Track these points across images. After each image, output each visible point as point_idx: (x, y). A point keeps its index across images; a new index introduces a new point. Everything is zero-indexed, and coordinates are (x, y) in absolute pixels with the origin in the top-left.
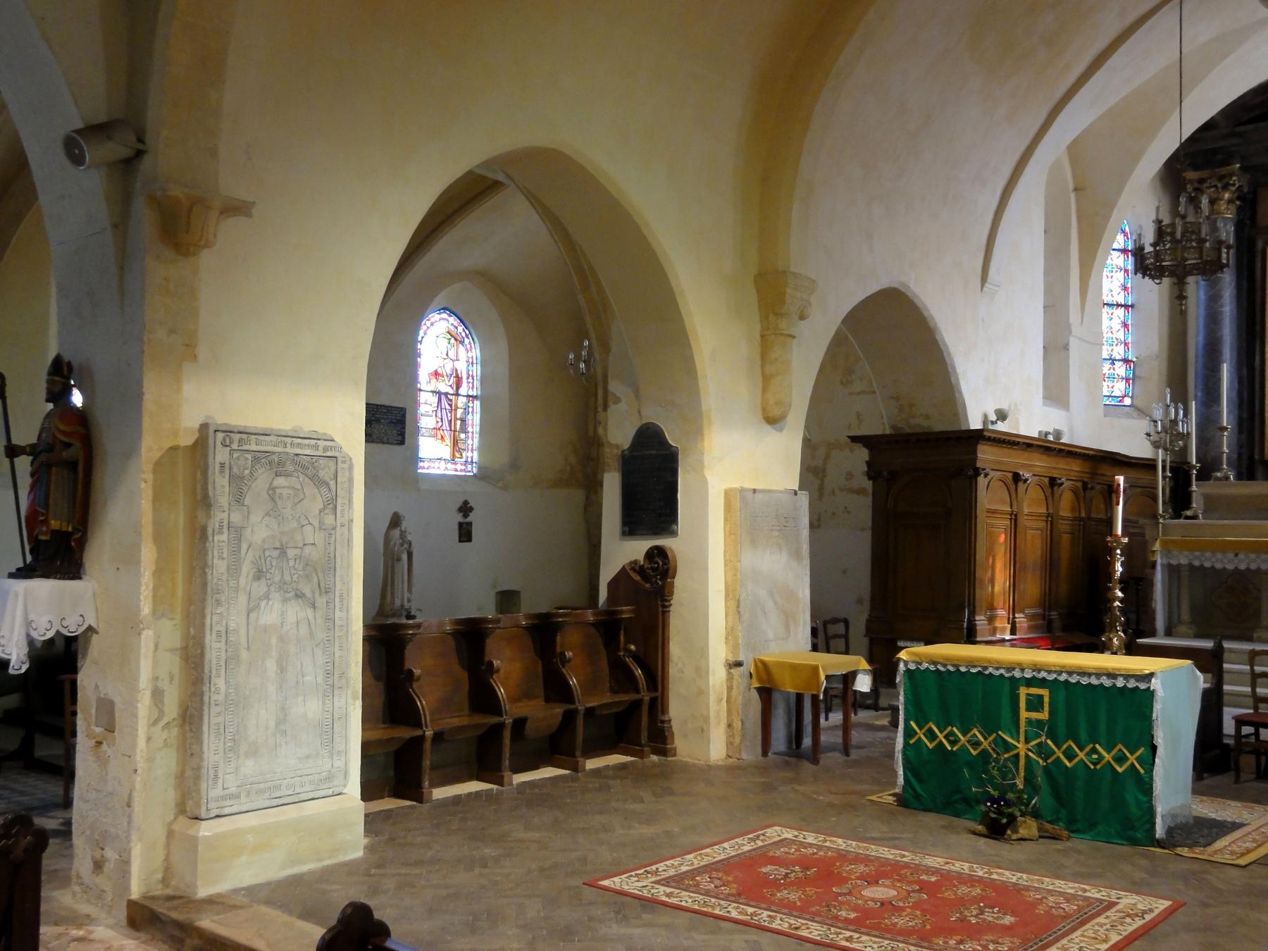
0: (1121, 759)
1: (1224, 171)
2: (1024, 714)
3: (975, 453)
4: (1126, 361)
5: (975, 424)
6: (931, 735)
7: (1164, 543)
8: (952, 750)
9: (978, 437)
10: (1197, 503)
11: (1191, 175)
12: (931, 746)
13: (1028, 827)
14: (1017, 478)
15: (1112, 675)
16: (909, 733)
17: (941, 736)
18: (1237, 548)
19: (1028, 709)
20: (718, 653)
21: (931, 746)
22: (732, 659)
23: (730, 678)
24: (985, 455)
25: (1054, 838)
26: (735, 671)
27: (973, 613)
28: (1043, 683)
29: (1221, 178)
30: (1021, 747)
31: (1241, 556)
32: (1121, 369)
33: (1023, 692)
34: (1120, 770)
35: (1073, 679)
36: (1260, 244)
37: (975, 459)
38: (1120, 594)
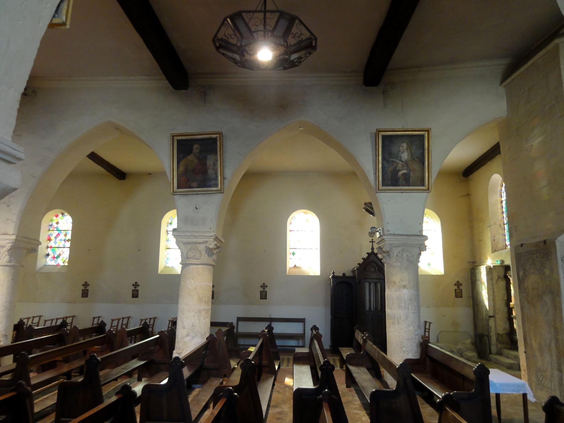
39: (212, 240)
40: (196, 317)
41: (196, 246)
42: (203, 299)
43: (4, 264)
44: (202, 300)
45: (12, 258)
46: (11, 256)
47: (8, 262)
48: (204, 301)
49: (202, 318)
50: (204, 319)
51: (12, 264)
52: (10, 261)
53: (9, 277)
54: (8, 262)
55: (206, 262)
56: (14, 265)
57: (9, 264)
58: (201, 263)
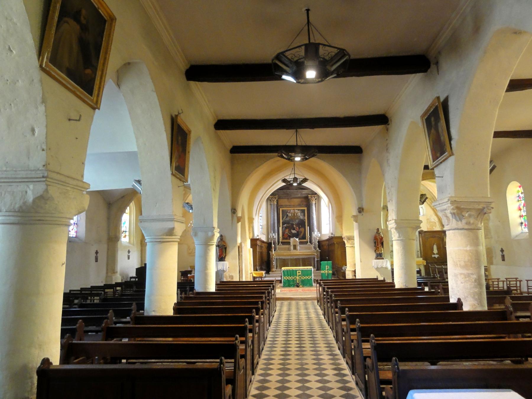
0: (309, 277)
1: (275, 196)
2: (298, 274)
3: (257, 242)
4: (261, 226)
5: (255, 238)
6: (286, 278)
7: (276, 255)
8: (290, 280)
9: (258, 239)
10: (277, 249)
11: (271, 197)
12: (286, 279)
13: (301, 286)
14: (259, 245)
15: (308, 268)
16: (284, 278)
17: (287, 278)
18: (286, 255)
19: (298, 273)
20: (249, 272)
21: (286, 279)
22: (250, 273)
23: (250, 275)
24: (258, 243)
25: (303, 287)
26: (251, 274)
27: (257, 267)
28: (300, 270)
29: (275, 197)
30: (298, 278)
31: (287, 256)
32: (261, 227)
33: (298, 271)
34: (309, 279)
35: (303, 269)
36: (279, 208)
37: (257, 243)
38: (274, 263)
39: (449, 205)
40: (453, 281)
41: (445, 213)
42: (458, 264)
43: (397, 239)
44: (457, 264)
45: (400, 235)
46: (399, 233)
47: (398, 238)
48: (459, 266)
49: (459, 282)
50: (462, 283)
51: (402, 238)
52: (399, 237)
53: (401, 247)
54: (398, 238)
55: (456, 227)
56: (402, 239)
57: (399, 239)
58: (450, 228)
